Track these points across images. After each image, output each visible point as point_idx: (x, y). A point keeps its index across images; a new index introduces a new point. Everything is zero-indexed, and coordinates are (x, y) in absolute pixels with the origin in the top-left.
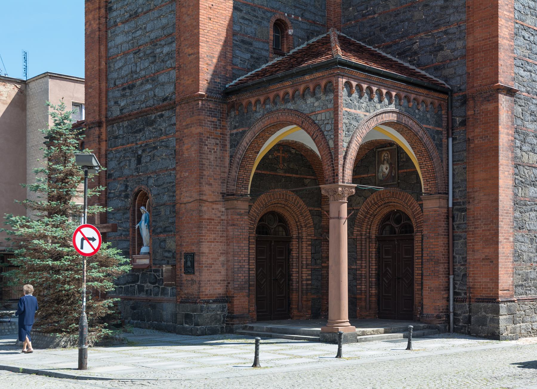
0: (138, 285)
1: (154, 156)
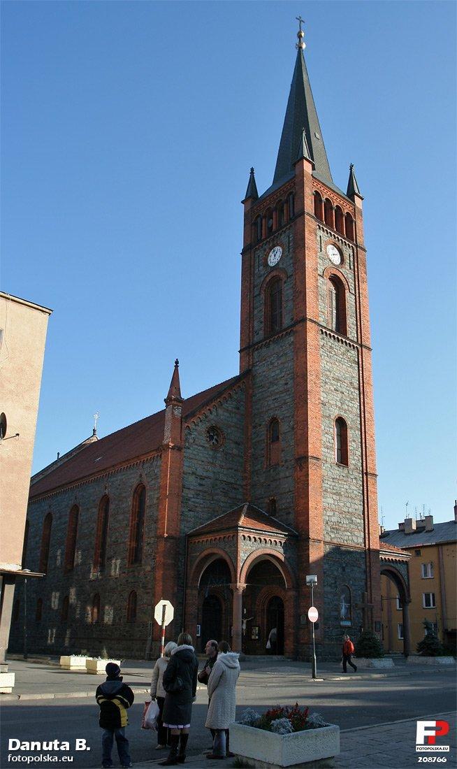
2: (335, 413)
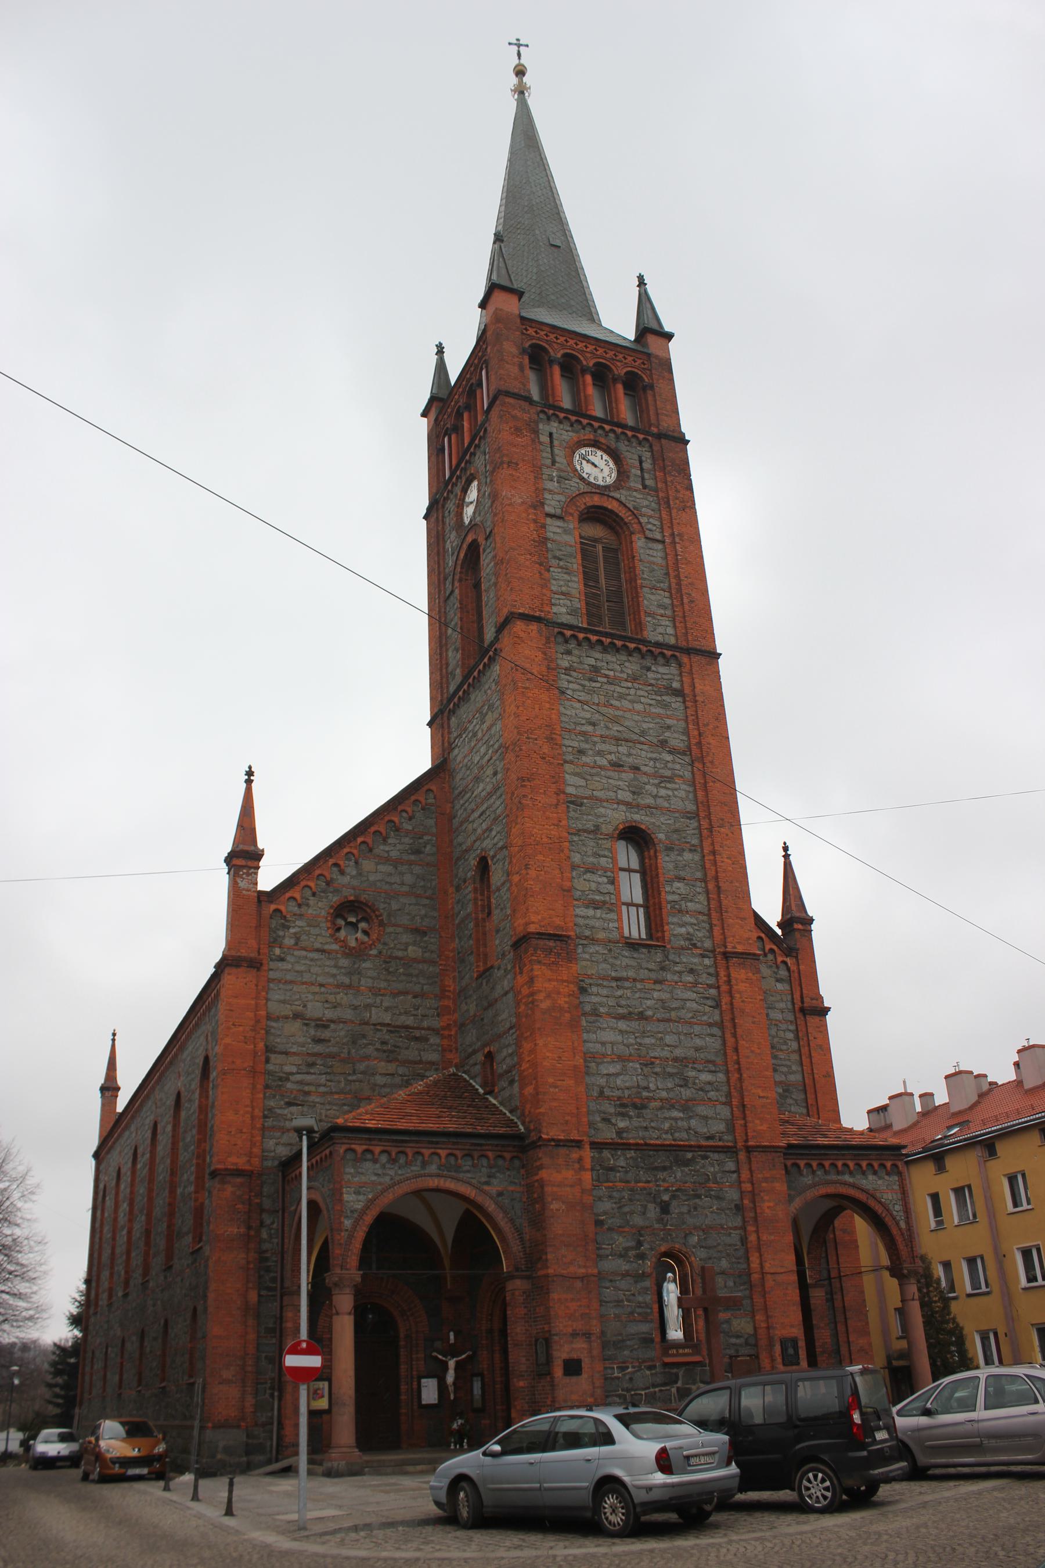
0: (678, 1389)
1: (695, 1208)
2: (617, 817)
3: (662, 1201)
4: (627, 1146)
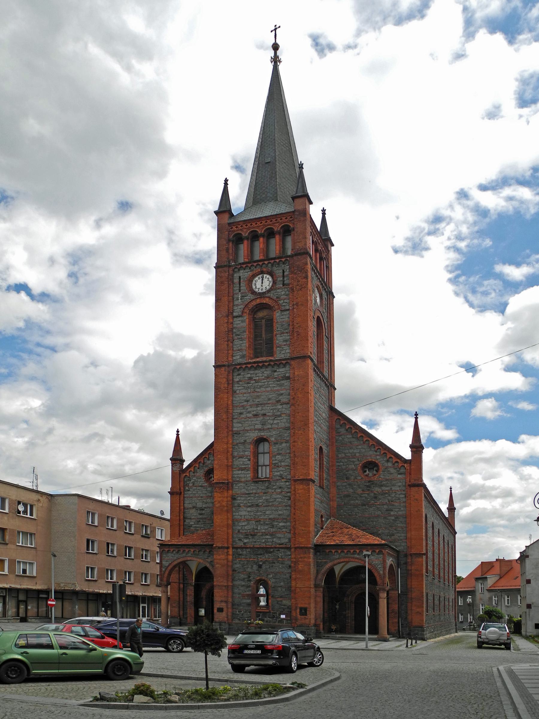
3: (259, 564)
4: (247, 548)
